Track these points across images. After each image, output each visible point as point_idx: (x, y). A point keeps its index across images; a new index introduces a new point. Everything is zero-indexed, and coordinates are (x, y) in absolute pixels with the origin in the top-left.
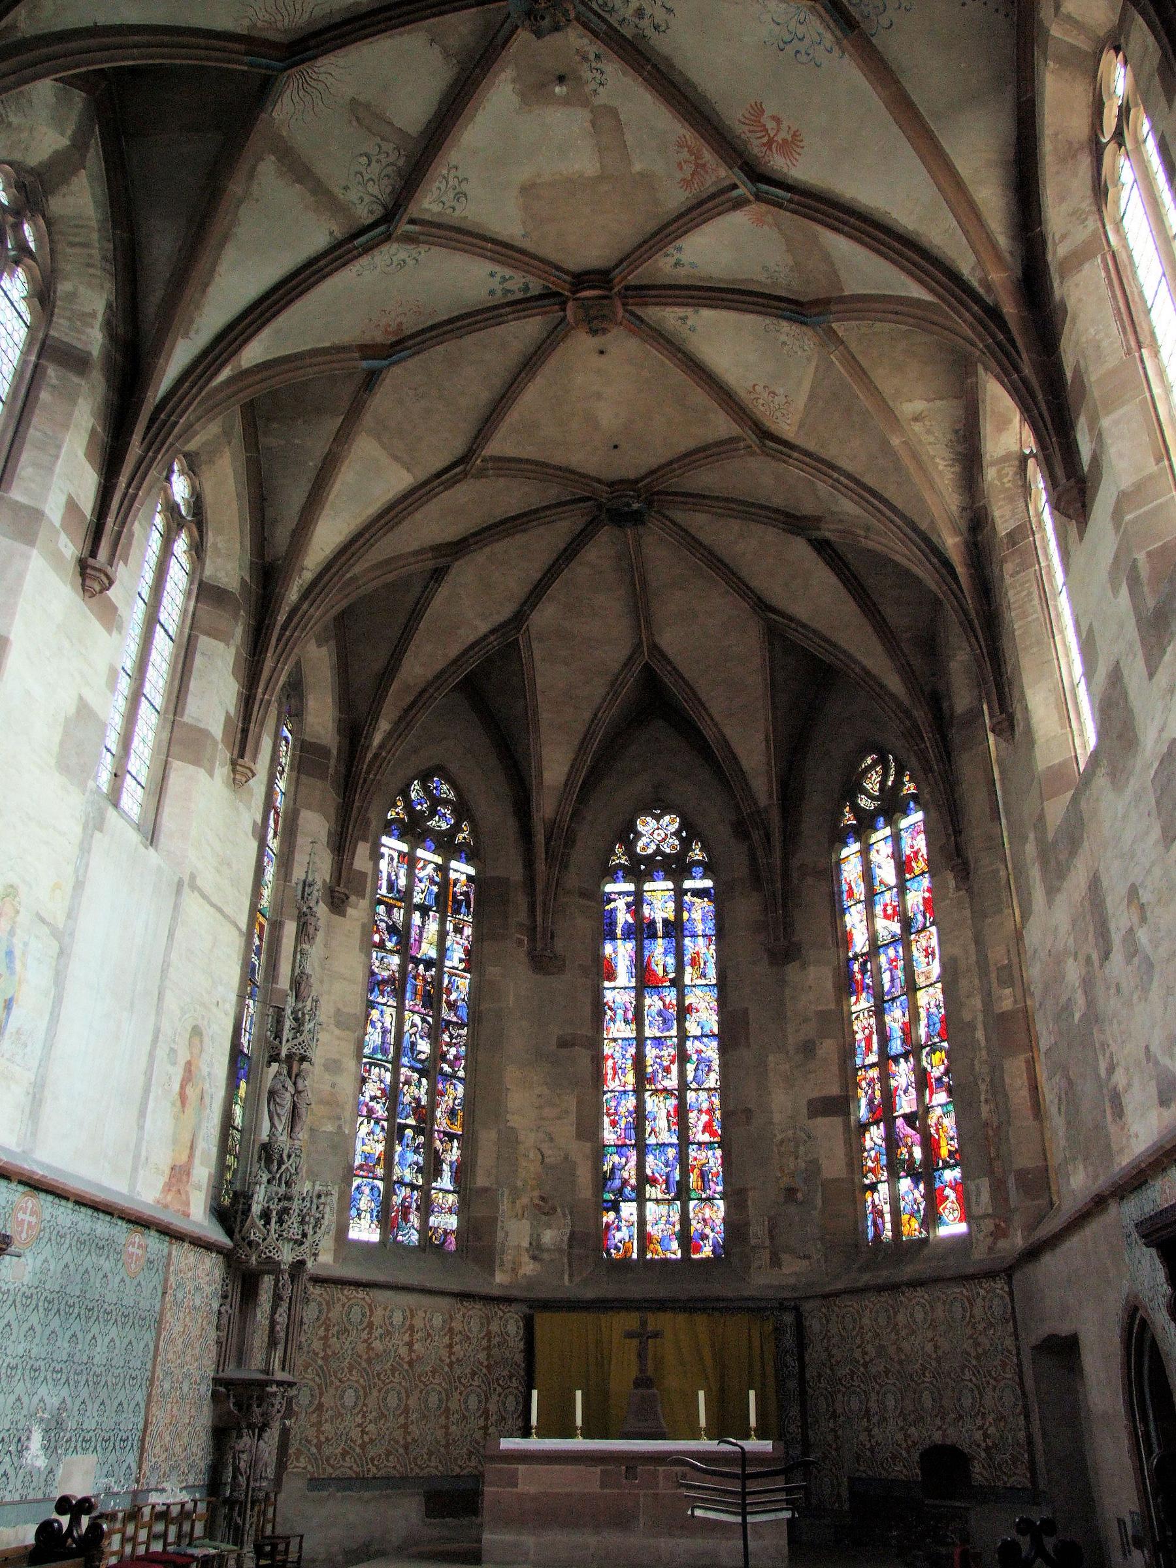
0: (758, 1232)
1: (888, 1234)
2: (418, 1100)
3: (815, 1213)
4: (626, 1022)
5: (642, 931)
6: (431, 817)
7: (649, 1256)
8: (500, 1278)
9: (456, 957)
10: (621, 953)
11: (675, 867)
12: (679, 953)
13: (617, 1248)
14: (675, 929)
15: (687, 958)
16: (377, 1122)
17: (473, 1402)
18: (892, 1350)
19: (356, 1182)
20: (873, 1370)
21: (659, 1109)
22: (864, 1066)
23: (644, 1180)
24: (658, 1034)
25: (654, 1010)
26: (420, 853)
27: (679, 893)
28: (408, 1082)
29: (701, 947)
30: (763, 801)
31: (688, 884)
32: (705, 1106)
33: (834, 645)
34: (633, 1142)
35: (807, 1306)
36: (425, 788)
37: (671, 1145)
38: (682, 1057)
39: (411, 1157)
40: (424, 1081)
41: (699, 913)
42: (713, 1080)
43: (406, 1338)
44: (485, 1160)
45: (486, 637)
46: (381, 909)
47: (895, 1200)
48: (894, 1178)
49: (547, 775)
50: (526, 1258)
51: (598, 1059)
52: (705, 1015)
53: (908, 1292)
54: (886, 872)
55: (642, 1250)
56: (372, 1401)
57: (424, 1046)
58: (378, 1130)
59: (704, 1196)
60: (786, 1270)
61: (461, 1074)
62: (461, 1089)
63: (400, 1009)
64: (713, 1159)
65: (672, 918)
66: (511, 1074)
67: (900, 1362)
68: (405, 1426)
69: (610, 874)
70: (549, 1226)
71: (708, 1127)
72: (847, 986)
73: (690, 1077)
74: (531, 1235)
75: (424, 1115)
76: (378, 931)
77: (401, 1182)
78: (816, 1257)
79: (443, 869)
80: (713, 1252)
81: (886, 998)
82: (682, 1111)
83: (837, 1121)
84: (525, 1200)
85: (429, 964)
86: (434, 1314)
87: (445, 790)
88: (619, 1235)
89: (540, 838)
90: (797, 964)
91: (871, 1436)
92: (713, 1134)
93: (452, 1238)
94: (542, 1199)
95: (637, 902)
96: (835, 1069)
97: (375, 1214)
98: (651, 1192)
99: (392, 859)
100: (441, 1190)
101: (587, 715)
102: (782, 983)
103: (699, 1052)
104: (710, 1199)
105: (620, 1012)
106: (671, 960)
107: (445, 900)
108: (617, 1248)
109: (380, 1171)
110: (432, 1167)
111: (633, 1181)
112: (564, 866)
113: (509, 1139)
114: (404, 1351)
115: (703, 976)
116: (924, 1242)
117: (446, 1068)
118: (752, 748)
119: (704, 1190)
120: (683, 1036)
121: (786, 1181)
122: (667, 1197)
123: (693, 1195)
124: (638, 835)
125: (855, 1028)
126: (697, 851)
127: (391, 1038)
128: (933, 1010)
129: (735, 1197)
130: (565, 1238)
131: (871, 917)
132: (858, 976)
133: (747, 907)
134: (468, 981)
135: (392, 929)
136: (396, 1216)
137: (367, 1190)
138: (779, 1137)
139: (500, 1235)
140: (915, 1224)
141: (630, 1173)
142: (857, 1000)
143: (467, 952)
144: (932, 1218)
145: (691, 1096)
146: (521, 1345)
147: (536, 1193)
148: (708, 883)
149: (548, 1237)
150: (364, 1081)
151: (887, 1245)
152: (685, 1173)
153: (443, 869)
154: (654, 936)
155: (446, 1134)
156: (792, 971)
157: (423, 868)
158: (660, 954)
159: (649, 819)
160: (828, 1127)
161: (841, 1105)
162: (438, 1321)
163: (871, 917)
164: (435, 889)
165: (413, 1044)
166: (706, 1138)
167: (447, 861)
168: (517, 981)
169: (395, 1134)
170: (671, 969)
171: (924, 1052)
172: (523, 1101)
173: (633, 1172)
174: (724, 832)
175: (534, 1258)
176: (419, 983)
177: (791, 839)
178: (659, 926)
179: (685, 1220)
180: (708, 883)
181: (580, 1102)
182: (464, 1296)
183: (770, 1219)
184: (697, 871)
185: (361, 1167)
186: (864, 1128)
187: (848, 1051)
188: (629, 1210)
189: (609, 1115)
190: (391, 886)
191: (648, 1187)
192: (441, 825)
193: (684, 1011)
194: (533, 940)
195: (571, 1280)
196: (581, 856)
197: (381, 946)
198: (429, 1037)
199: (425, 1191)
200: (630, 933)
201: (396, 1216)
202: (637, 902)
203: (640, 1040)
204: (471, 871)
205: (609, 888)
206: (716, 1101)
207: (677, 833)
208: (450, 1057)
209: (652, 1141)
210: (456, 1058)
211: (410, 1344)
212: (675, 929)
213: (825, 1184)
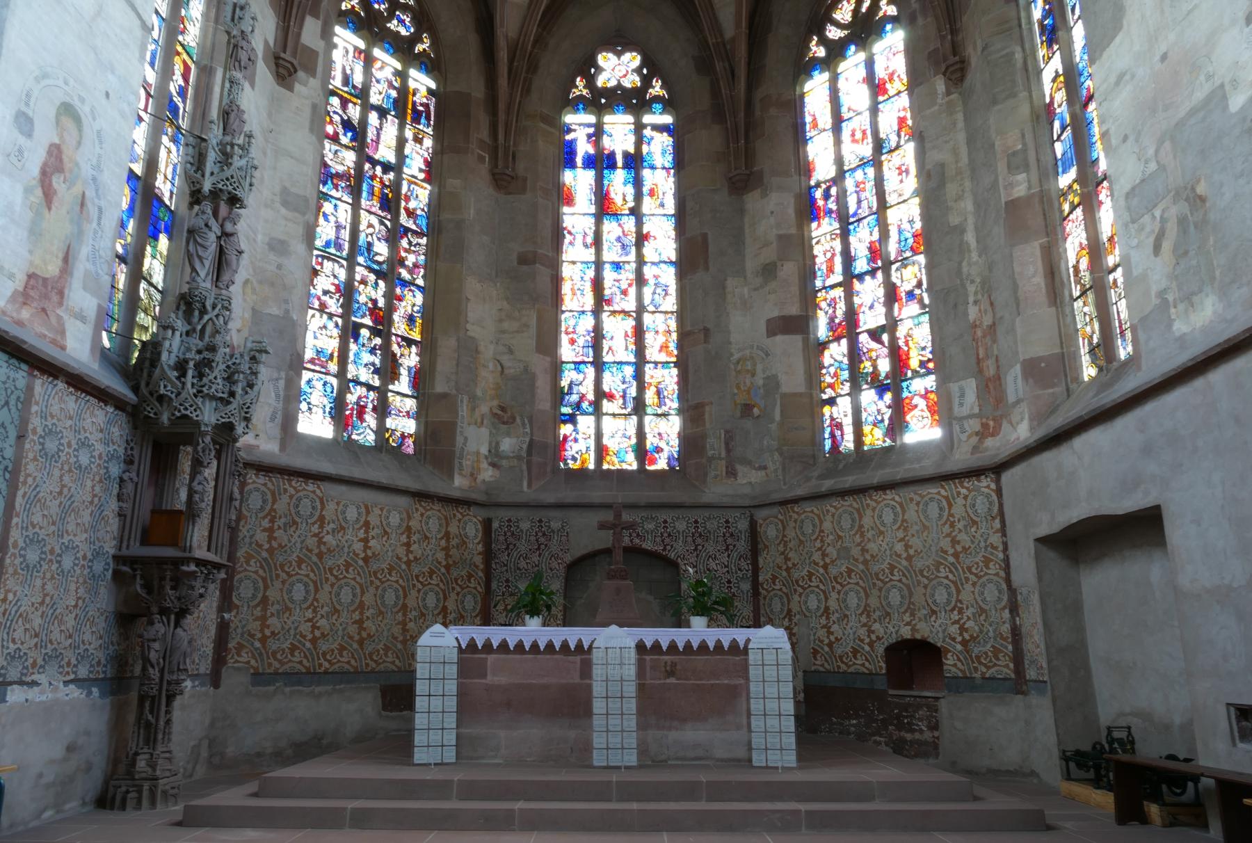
0: (715, 445)
1: (848, 443)
2: (375, 302)
3: (774, 426)
4: (586, 246)
5: (601, 162)
6: (390, 19)
7: (605, 466)
8: (458, 481)
9: (415, 165)
10: (580, 181)
11: (634, 101)
12: (638, 183)
13: (574, 459)
14: (634, 162)
15: (645, 190)
16: (331, 316)
18: (856, 552)
19: (306, 375)
20: (833, 571)
21: (617, 330)
22: (824, 288)
23: (601, 395)
24: (617, 259)
25: (612, 237)
26: (377, 52)
27: (639, 128)
28: (364, 282)
29: (661, 182)
30: (729, 31)
31: (647, 119)
32: (662, 328)
34: (591, 359)
35: (760, 515)
37: (628, 363)
38: (640, 281)
39: (367, 357)
40: (381, 283)
41: (659, 148)
42: (670, 303)
43: (361, 534)
44: (444, 366)
46: (335, 101)
50: (484, 465)
51: (557, 280)
52: (663, 242)
53: (878, 496)
56: (323, 596)
57: (382, 249)
58: (331, 325)
59: (660, 412)
60: (741, 480)
61: (420, 282)
62: (419, 299)
63: (356, 206)
64: (668, 378)
65: (632, 150)
66: (472, 285)
67: (865, 562)
68: (360, 622)
70: (508, 435)
71: (664, 348)
72: (810, 211)
73: (647, 301)
74: (490, 444)
75: (382, 321)
76: (331, 122)
77: (357, 382)
78: (771, 467)
79: (402, 75)
80: (668, 464)
81: (852, 220)
83: (797, 339)
85: (387, 167)
86: (393, 511)
88: (576, 447)
89: (503, 55)
90: (757, 193)
91: (830, 633)
92: (669, 354)
93: (410, 441)
94: (503, 409)
95: (598, 133)
96: (795, 289)
97: (328, 409)
98: (607, 406)
99: (347, 52)
100: (398, 393)
102: (742, 211)
103: (656, 277)
104: (665, 415)
105: (579, 239)
106: (630, 190)
107: (402, 106)
108: (574, 459)
109: (333, 367)
110: (389, 370)
111: (591, 397)
112: (527, 91)
113: (469, 349)
114: (358, 547)
115: (662, 205)
116: (889, 449)
117: (405, 274)
119: (659, 406)
120: (641, 262)
121: (741, 399)
122: (624, 411)
123: (649, 410)
124: (599, 70)
125: (815, 252)
126: (657, 88)
127: (346, 234)
128: (906, 226)
129: (691, 410)
130: (525, 446)
132: (821, 203)
133: (709, 138)
134: (427, 192)
135: (347, 125)
136: (351, 414)
137: (319, 385)
138: (736, 356)
139: (459, 440)
141: (588, 389)
142: (819, 225)
144: (897, 424)
145: (647, 319)
146: (480, 548)
147: (495, 403)
148: (668, 119)
149: (507, 445)
150: (315, 273)
151: (848, 455)
152: (641, 387)
154: (612, 166)
155: (403, 338)
156: (752, 201)
157: (381, 68)
159: (610, 55)
160: (789, 343)
161: (799, 324)
162: (395, 519)
163: (838, 142)
164: (394, 94)
165: (370, 245)
166: (663, 357)
168: (477, 198)
169: (350, 332)
170: (630, 198)
171: (894, 267)
172: (483, 312)
173: (591, 387)
175: (493, 465)
176: (377, 184)
177: (755, 74)
180: (668, 119)
181: (540, 319)
182: (421, 496)
183: (727, 432)
185: (312, 361)
186: (823, 346)
187: (809, 272)
188: (586, 423)
189: (567, 333)
190: (346, 80)
191: (605, 402)
193: (641, 239)
195: (529, 485)
197: (335, 138)
198: (387, 240)
199: (382, 393)
200: (590, 162)
201: (351, 414)
203: (599, 265)
204: (433, 85)
205: (569, 118)
206: (673, 325)
207: (638, 71)
208: (409, 263)
209: (607, 358)
210: (416, 265)
211: (365, 541)
212: (634, 162)
213: (784, 396)
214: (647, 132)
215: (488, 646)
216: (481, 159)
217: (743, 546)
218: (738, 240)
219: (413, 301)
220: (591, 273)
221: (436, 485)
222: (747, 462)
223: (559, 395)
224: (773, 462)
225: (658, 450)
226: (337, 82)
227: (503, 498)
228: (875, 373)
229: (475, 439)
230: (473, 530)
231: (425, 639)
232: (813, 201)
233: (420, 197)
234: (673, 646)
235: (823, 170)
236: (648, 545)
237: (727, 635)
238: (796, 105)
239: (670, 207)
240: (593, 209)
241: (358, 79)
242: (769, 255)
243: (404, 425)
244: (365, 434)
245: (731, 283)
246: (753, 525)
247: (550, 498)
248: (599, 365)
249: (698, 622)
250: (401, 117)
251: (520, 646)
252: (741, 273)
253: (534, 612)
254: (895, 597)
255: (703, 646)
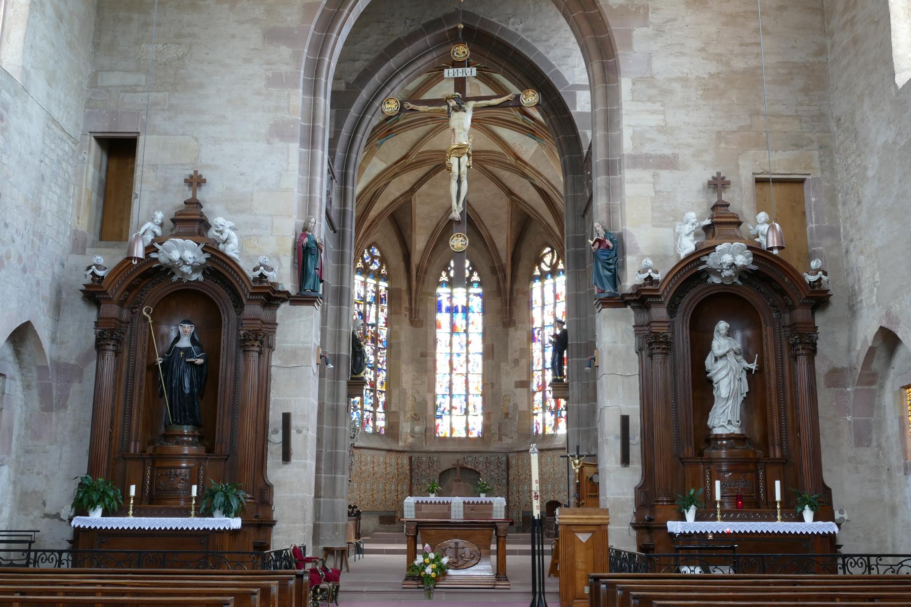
1: (540, 432)
5: (452, 310)
8: (401, 444)
10: (443, 318)
12: (467, 319)
14: (466, 310)
15: (470, 322)
17: (393, 487)
23: (452, 407)
27: (468, 295)
29: (477, 318)
30: (504, 262)
31: (472, 290)
33: (537, 213)
35: (511, 455)
36: (369, 252)
38: (468, 361)
41: (476, 304)
42: (480, 370)
44: (394, 401)
45: (398, 198)
47: (544, 420)
48: (544, 411)
49: (417, 247)
52: (477, 345)
54: (549, 298)
55: (451, 432)
56: (362, 487)
62: (385, 373)
69: (440, 284)
71: (477, 388)
79: (377, 286)
82: (467, 382)
83: (525, 390)
84: (409, 415)
85: (373, 325)
86: (381, 457)
87: (376, 252)
89: (414, 273)
95: (451, 297)
96: (525, 370)
101: (435, 223)
102: (507, 335)
106: (464, 322)
109: (359, 406)
110: (375, 405)
111: (448, 408)
113: (403, 393)
116: (552, 435)
118: (502, 240)
120: (468, 353)
121: (504, 411)
129: (487, 414)
131: (543, 314)
132: (536, 336)
133: (496, 303)
140: (551, 428)
143: (386, 319)
144: (556, 427)
145: (469, 376)
149: (417, 429)
152: (467, 405)
153: (377, 286)
154: (457, 311)
156: (511, 330)
158: (459, 318)
161: (525, 384)
162: (381, 459)
163: (543, 314)
167: (378, 282)
168: (405, 330)
174: (486, 270)
176: (369, 334)
178: (460, 309)
179: (467, 424)
180: (480, 290)
184: (476, 285)
186: (534, 393)
187: (530, 364)
188: (446, 418)
192: (374, 267)
193: (468, 343)
194: (411, 313)
196: (430, 278)
199: (374, 413)
202: (451, 297)
203: (451, 355)
204: (386, 285)
213: (520, 412)
214: (471, 296)
215: (422, 502)
216: (406, 315)
217: (504, 466)
218: (505, 346)
219: (383, 375)
220: (448, 358)
221: (394, 446)
222: (507, 435)
223: (436, 408)
224: (515, 436)
225: (474, 429)
226: (356, 298)
227: (416, 449)
228: (550, 407)
229: (406, 427)
230: (406, 461)
231: (406, 501)
232: (534, 334)
233: (383, 334)
234: (473, 502)
235: (537, 324)
236: (469, 466)
237: (488, 499)
238: (528, 294)
239: (480, 330)
240: (449, 330)
241: (362, 295)
242: (516, 355)
243: (381, 424)
244: (369, 429)
245: (502, 365)
246: (508, 458)
247: (433, 449)
248: (451, 396)
249: (483, 495)
250: (377, 304)
251: (427, 502)
252: (506, 360)
253: (432, 492)
254: (550, 487)
255: (482, 503)
